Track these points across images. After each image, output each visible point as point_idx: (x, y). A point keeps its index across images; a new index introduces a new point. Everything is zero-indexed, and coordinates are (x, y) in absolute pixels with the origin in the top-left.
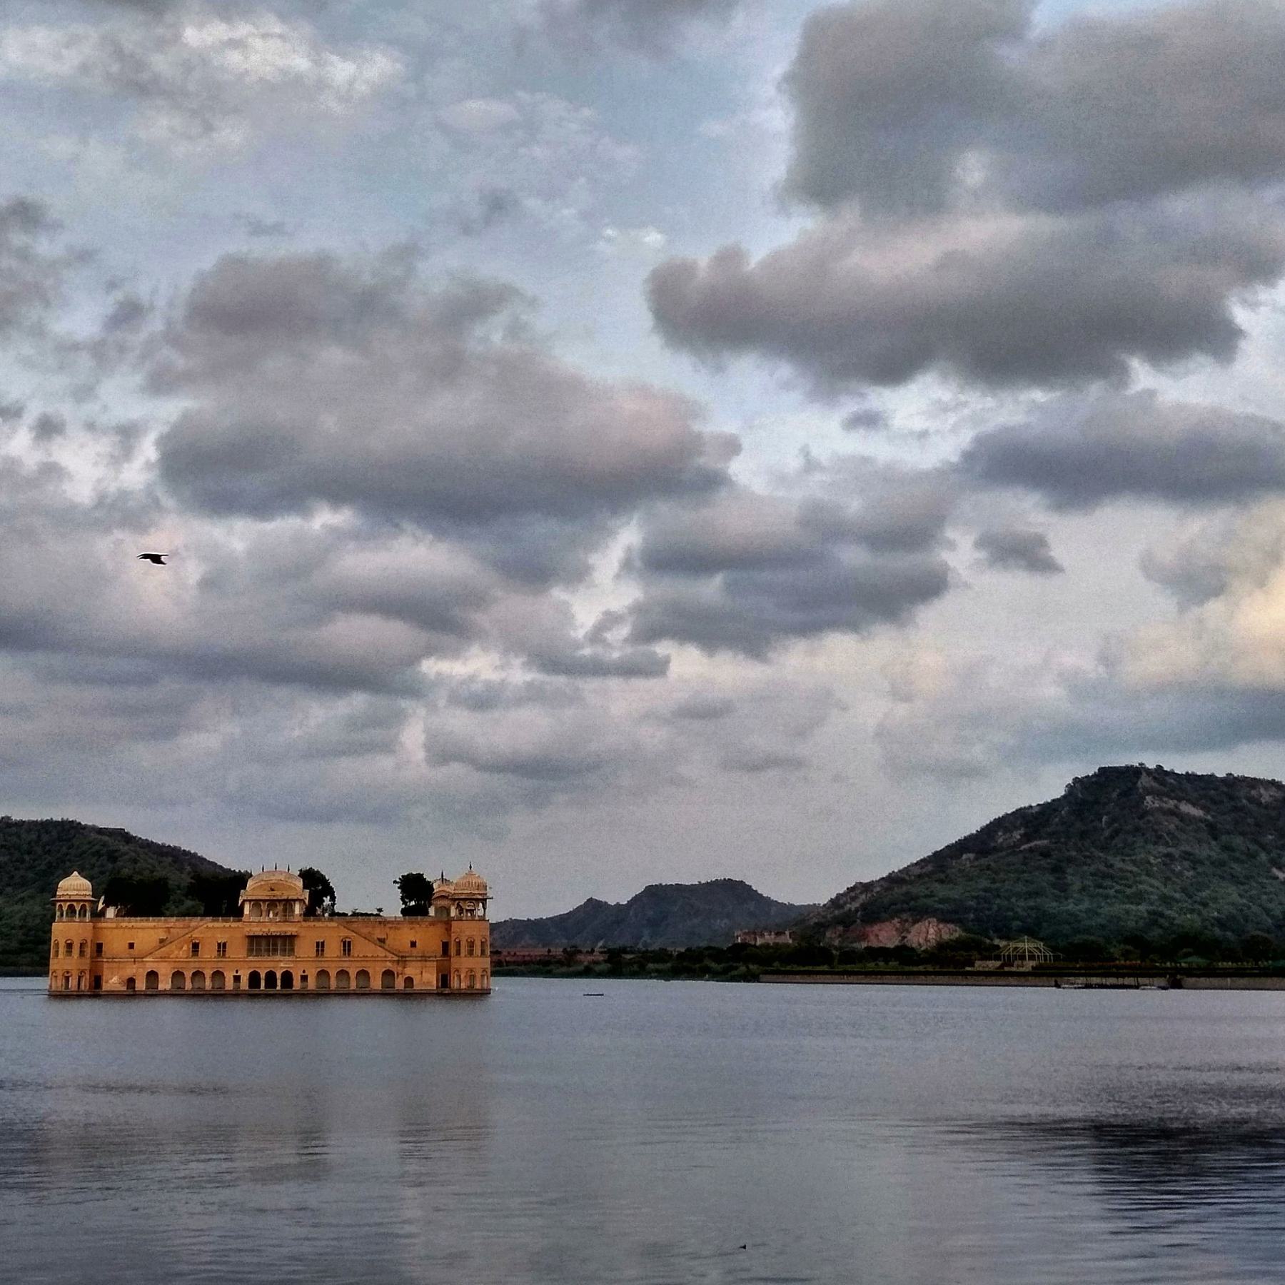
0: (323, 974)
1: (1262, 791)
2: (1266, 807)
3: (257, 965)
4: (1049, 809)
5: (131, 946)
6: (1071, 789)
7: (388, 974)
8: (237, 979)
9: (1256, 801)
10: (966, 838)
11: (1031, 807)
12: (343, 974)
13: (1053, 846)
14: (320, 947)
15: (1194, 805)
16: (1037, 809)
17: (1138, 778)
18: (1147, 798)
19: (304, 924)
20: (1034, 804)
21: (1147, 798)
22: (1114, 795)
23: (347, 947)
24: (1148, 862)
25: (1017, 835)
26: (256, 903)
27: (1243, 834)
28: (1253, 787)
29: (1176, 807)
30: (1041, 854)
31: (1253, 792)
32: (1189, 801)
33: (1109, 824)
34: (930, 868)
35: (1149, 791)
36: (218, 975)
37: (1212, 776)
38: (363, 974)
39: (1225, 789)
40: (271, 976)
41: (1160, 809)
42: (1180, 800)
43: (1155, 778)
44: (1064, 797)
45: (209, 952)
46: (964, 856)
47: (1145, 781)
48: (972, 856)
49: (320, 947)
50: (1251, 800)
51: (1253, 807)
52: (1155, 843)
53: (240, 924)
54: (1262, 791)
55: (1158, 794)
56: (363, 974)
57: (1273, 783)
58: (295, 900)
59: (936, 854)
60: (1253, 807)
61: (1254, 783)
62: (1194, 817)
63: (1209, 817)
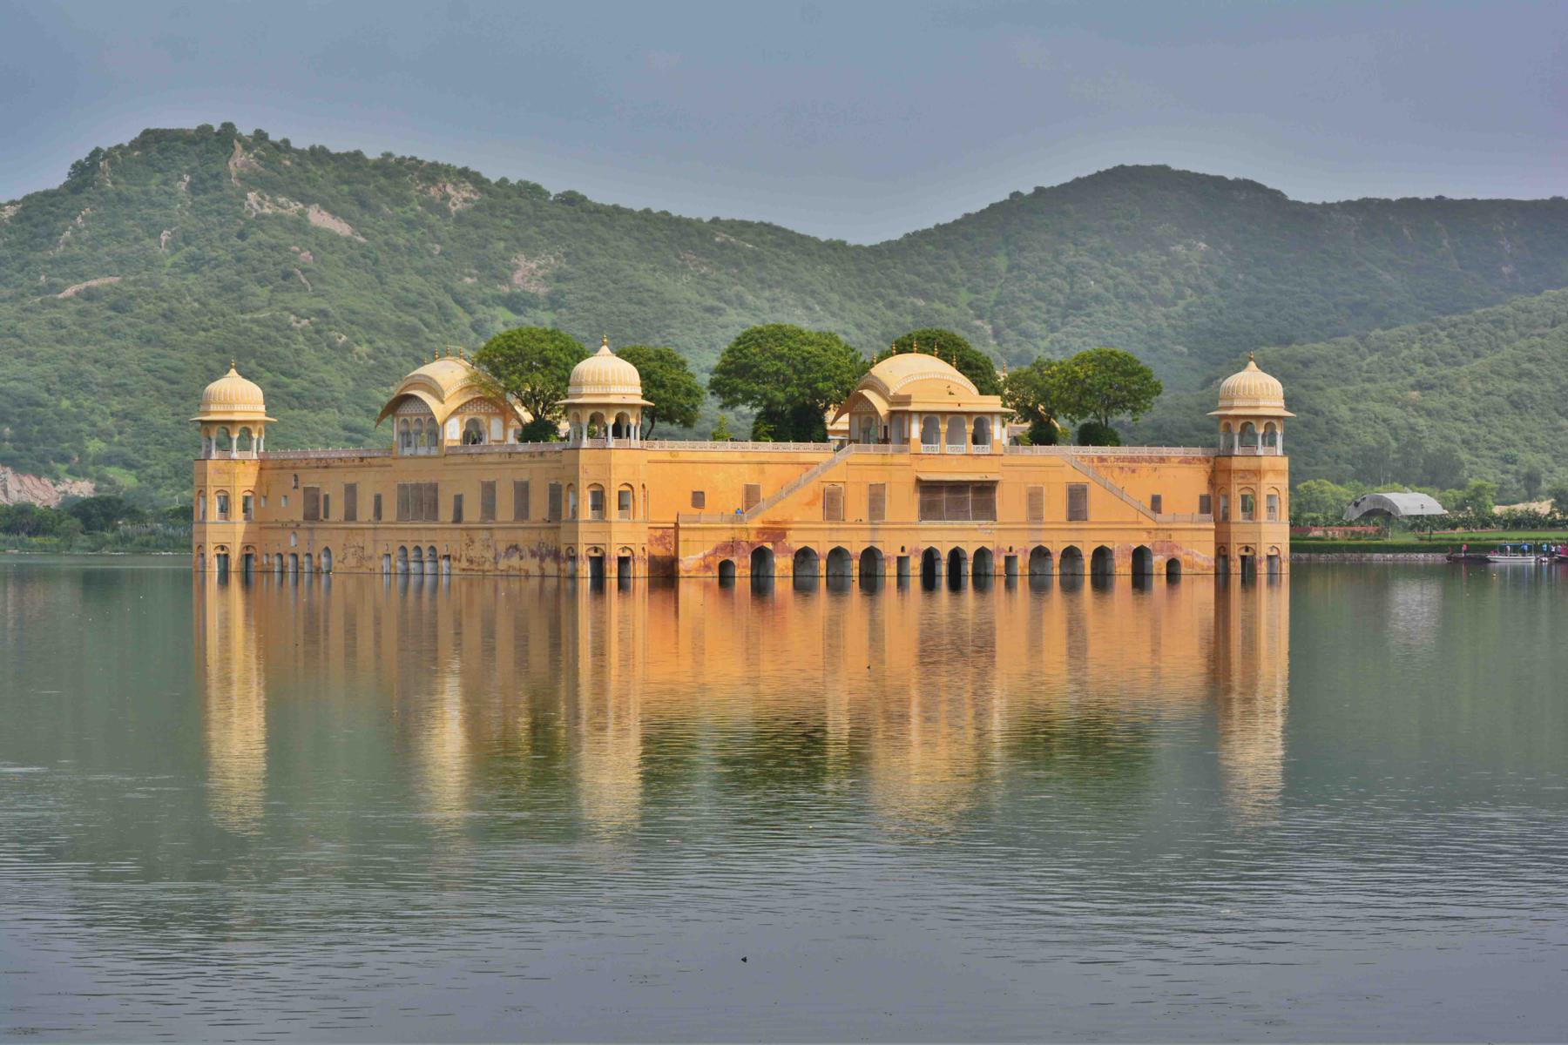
0: (1040, 554)
1: (450, 189)
2: (460, 219)
3: (935, 536)
5: (698, 499)
6: (84, 173)
7: (1140, 555)
8: (902, 561)
9: (442, 211)
12: (1071, 554)
13: (132, 290)
14: (1035, 500)
15: (334, 214)
19: (1007, 460)
23: (1077, 501)
24: (289, 327)
26: (930, 419)
27: (424, 272)
29: (302, 214)
30: (114, 307)
31: (433, 191)
32: (325, 206)
35: (251, 181)
36: (871, 556)
38: (1101, 554)
39: (383, 181)
40: (956, 556)
41: (279, 219)
42: (307, 200)
43: (258, 156)
45: (856, 507)
50: (429, 205)
51: (432, 218)
53: (902, 459)
54: (450, 189)
55: (268, 187)
56: (1101, 554)
57: (464, 173)
58: (992, 414)
61: (433, 173)
62: (335, 237)
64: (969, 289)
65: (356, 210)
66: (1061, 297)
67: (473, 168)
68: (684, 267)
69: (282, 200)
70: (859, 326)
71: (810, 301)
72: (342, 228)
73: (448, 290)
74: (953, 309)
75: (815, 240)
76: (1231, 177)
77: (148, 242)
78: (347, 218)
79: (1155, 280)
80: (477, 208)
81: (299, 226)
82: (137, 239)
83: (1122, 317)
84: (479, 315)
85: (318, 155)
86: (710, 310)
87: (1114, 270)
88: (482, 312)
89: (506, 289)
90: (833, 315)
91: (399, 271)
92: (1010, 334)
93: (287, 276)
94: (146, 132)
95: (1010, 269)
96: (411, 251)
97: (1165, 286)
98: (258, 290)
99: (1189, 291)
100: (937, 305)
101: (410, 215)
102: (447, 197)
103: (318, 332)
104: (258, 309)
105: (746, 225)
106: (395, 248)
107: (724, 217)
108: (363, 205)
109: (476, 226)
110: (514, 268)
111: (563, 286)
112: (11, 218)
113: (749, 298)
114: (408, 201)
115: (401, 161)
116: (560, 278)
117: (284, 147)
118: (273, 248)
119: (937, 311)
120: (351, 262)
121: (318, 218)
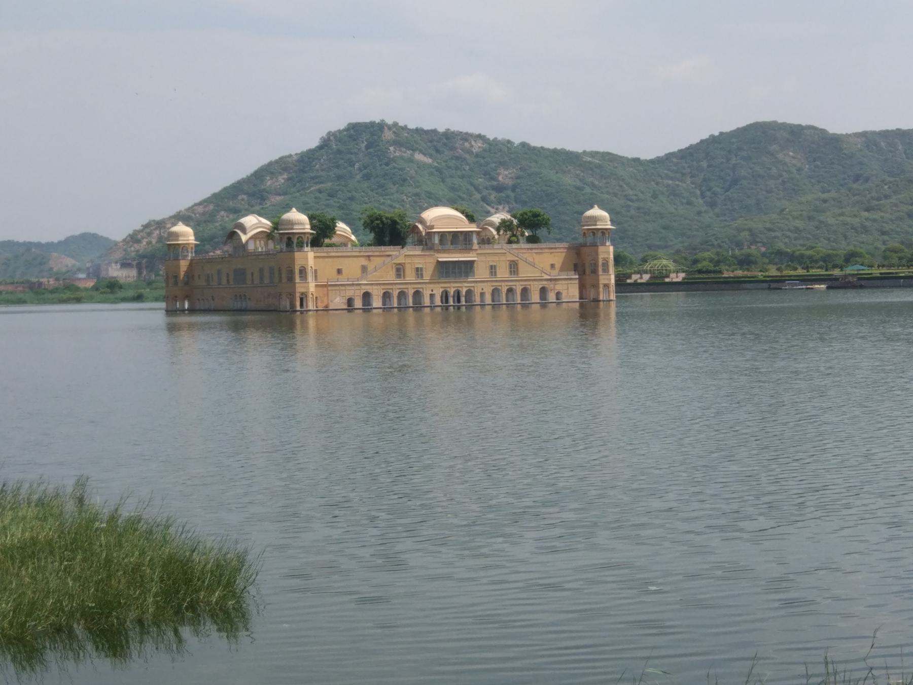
1: (473, 143)
2: (477, 156)
4: (307, 159)
9: (469, 152)
10: (239, 182)
11: (290, 156)
14: (493, 269)
15: (425, 154)
16: (295, 158)
17: (382, 132)
18: (392, 148)
20: (293, 153)
21: (392, 148)
22: (363, 146)
25: (282, 179)
27: (463, 177)
28: (467, 140)
31: (467, 144)
32: (421, 152)
33: (360, 170)
34: (211, 207)
37: (434, 131)
41: (402, 158)
42: (414, 150)
43: (394, 132)
44: (320, 148)
46: (240, 197)
47: (388, 135)
48: (245, 197)
49: (493, 269)
51: (467, 156)
52: (402, 185)
55: (397, 143)
57: (480, 137)
59: (215, 196)
60: (467, 156)
61: (466, 137)
62: (425, 164)
63: (436, 164)
64: (691, 177)
65: (433, 153)
66: (728, 178)
67: (483, 134)
68: (569, 171)
69: (404, 149)
70: (642, 193)
71: (621, 183)
72: (428, 160)
73: (472, 184)
74: (684, 185)
75: (627, 158)
76: (804, 124)
77: (349, 168)
78: (431, 156)
79: (770, 169)
80: (485, 150)
81: (411, 160)
82: (345, 168)
83: (756, 185)
84: (484, 194)
85: (419, 131)
86: (578, 188)
87: (752, 165)
88: (485, 192)
89: (495, 183)
90: (632, 189)
91: (451, 176)
92: (708, 193)
93: (404, 180)
94: (349, 124)
95: (709, 166)
96: (457, 168)
97: (774, 171)
98: (392, 186)
99: (784, 173)
100: (677, 183)
101: (457, 154)
102: (472, 146)
103: (415, 202)
104: (392, 194)
105: (597, 153)
106: (450, 167)
107: (588, 149)
108: (437, 151)
109: (484, 158)
110: (499, 174)
111: (519, 181)
112: (298, 161)
113: (597, 183)
114: (455, 148)
115: (453, 133)
116: (518, 178)
117: (405, 128)
118: (399, 169)
119: (678, 185)
120: (431, 174)
121: (419, 157)
